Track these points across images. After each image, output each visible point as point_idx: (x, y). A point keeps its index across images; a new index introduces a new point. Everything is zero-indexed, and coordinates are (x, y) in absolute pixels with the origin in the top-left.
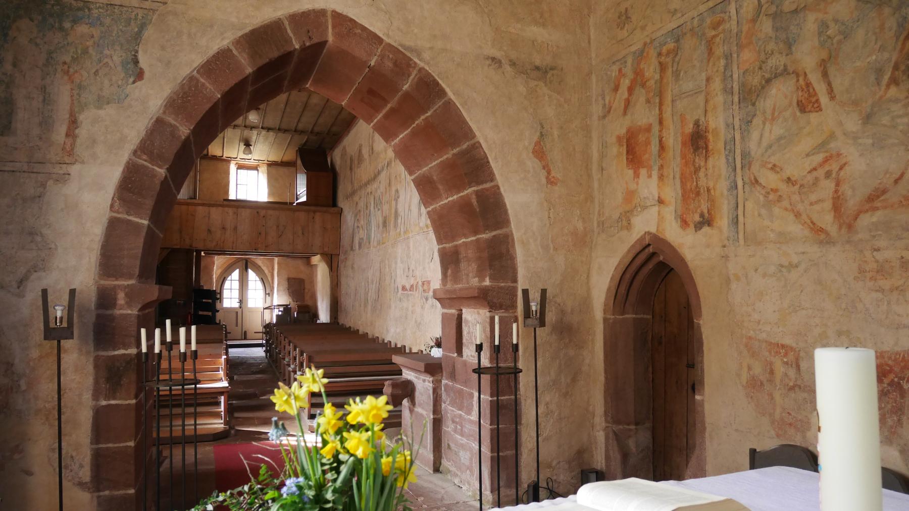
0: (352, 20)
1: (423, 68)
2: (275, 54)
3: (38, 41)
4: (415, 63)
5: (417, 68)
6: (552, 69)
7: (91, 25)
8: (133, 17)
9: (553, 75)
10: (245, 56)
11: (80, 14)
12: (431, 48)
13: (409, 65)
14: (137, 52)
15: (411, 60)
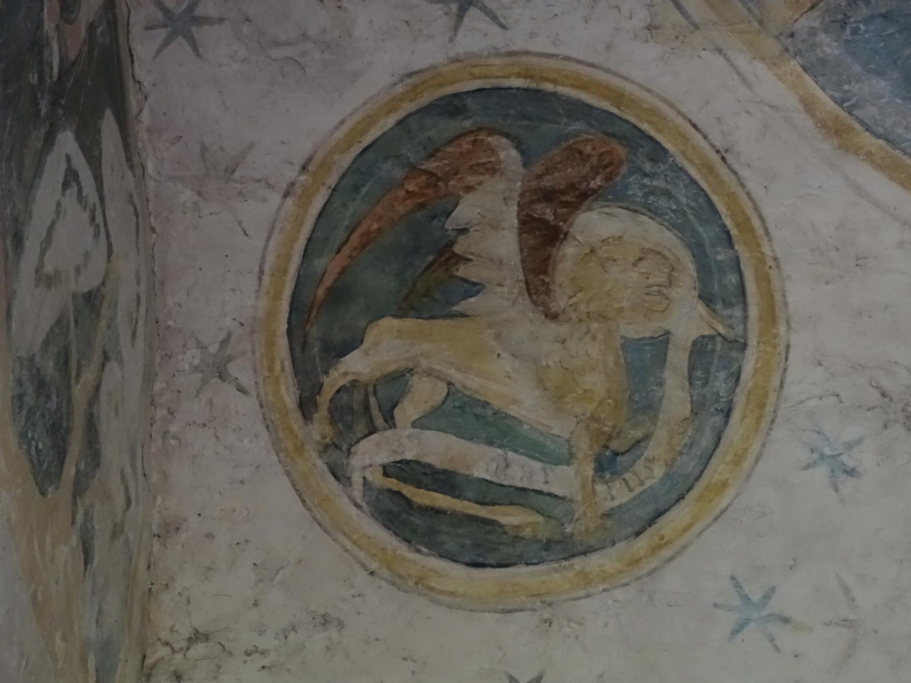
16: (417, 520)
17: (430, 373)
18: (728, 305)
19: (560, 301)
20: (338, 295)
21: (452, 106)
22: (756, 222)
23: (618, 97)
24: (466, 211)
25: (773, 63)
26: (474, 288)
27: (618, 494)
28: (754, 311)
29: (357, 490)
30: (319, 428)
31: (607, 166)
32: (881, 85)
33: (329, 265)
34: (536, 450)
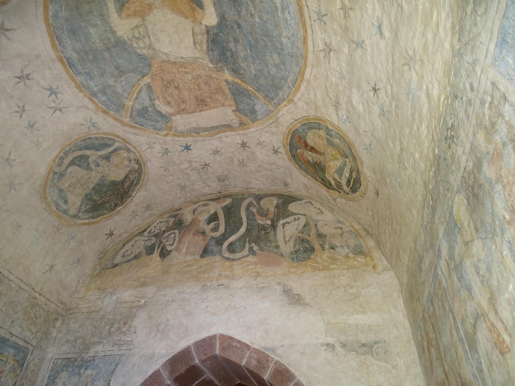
0: (232, 338)
1: (278, 361)
2: (182, 369)
3: (67, 383)
4: (273, 358)
5: (274, 362)
6: (375, 343)
7: (93, 369)
8: (113, 360)
9: (378, 348)
10: (167, 373)
11: (89, 364)
12: (282, 346)
13: (268, 361)
14: (110, 381)
15: (269, 356)
16: (354, 188)
17: (333, 174)
18: (321, 126)
19: (322, 151)
20: (323, 180)
21: (294, 156)
22: (307, 118)
23: (289, 134)
24: (310, 159)
25: (280, 111)
26: (320, 162)
27: (350, 157)
28: (321, 123)
29: (351, 194)
30: (342, 192)
31: (300, 137)
32: (281, 94)
33: (319, 179)
34: (345, 165)
